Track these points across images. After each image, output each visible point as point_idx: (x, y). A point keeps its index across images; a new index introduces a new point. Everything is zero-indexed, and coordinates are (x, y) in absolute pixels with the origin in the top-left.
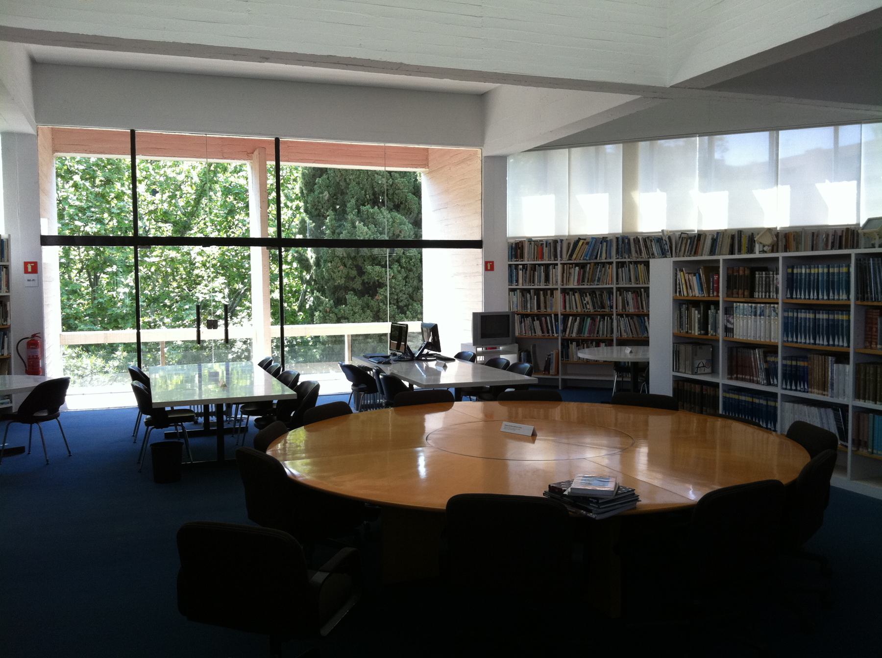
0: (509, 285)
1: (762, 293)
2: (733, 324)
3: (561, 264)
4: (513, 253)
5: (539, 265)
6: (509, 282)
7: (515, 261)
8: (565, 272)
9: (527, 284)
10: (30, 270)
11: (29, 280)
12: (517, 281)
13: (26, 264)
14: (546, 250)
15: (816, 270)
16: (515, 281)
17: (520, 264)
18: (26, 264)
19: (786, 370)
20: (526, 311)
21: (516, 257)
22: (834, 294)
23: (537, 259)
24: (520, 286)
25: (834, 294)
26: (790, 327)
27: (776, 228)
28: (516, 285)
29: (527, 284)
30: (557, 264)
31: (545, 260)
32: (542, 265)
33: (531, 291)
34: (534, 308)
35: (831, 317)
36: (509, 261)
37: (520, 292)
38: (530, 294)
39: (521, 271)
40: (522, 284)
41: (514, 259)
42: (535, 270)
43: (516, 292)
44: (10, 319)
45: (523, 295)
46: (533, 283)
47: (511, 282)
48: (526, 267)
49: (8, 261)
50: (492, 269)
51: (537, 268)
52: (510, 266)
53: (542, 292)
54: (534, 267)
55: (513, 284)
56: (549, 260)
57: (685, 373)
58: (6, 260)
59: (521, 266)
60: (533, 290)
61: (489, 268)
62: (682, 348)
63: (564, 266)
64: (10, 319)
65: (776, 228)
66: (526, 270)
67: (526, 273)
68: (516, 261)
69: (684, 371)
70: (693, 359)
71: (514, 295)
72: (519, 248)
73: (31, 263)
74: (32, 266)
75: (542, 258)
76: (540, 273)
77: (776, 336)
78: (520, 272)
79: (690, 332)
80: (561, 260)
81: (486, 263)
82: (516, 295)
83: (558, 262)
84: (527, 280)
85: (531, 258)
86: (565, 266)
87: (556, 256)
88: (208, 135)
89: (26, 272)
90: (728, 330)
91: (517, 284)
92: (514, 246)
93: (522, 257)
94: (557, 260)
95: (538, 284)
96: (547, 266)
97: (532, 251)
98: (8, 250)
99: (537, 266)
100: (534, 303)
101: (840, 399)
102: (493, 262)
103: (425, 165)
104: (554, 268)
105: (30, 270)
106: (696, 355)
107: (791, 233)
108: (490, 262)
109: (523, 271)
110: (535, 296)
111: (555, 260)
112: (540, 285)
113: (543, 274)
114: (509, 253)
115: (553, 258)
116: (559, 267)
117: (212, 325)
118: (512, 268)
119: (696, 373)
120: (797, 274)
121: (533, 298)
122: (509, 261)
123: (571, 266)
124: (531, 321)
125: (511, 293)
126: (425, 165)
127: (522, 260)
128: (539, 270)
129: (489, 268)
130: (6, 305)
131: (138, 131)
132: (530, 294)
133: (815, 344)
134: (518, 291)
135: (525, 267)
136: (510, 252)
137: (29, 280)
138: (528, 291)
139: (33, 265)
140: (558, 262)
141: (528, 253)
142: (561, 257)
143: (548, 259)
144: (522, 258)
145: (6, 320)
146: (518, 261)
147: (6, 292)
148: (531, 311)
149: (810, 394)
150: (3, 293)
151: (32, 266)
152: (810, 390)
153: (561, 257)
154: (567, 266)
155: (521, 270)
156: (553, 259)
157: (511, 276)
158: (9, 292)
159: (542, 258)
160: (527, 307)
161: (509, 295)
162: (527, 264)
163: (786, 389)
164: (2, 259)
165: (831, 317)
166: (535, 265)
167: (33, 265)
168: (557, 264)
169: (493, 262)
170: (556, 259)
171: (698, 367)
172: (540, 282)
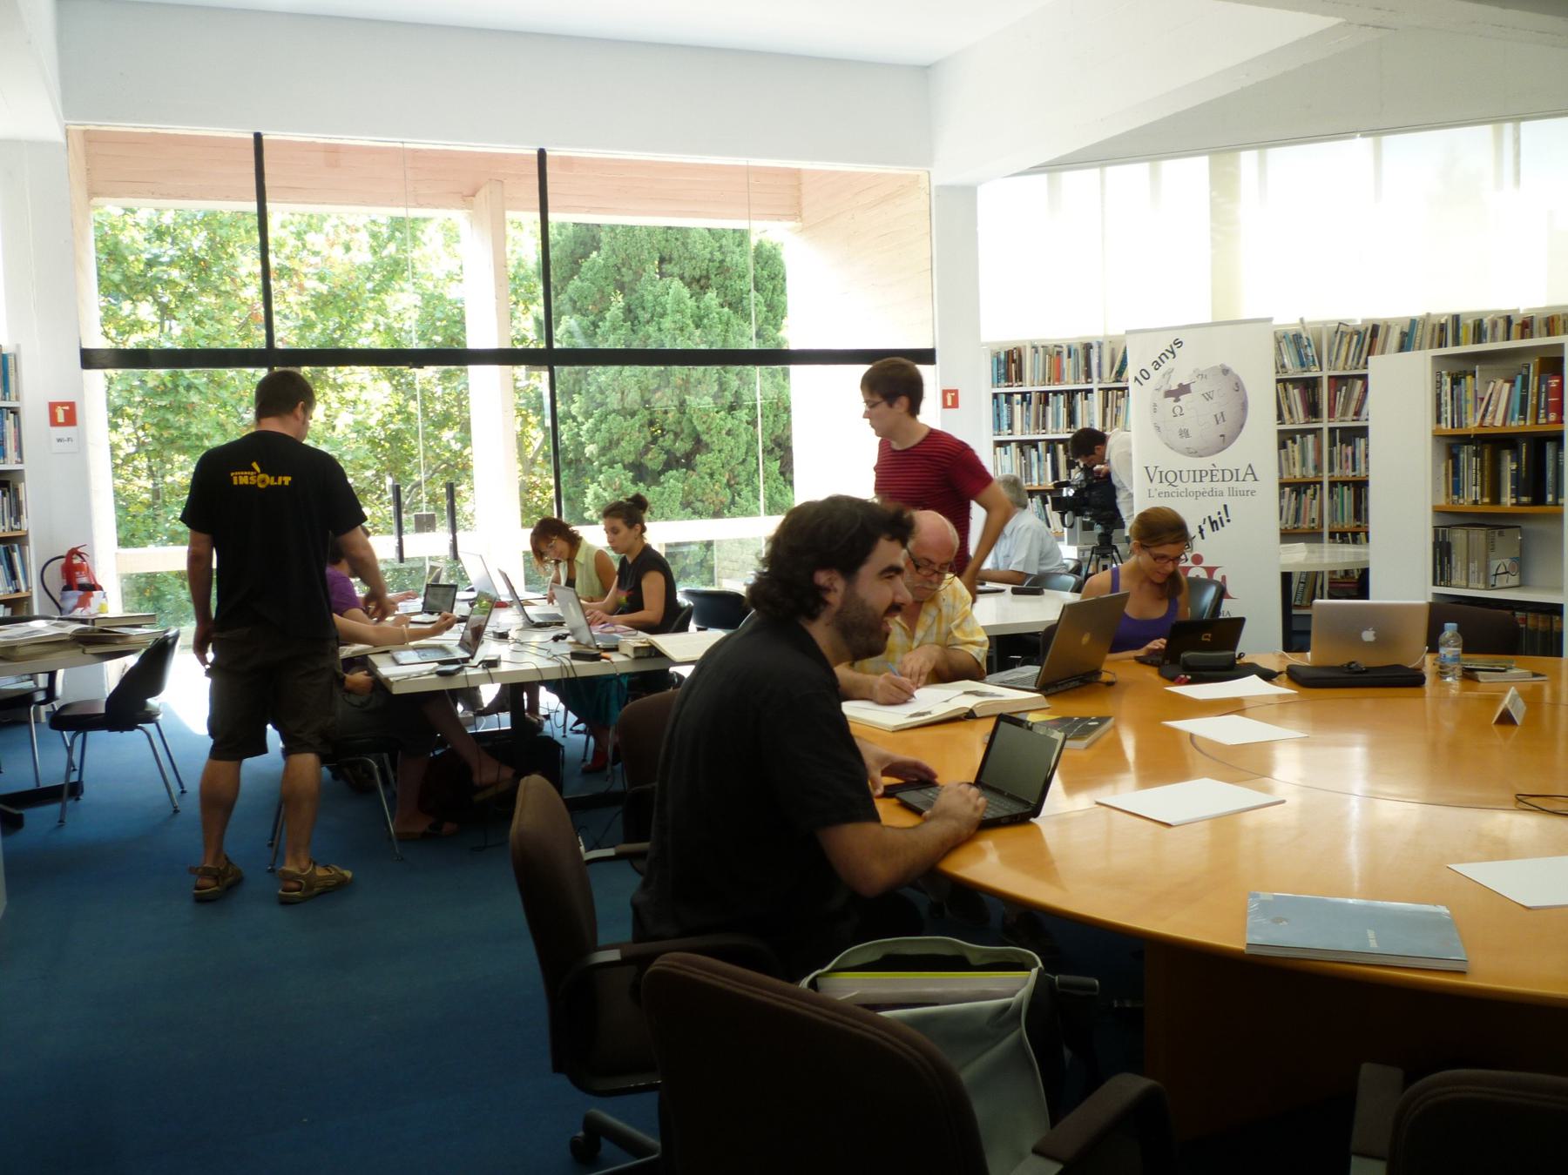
0: (994, 435)
3: (1100, 389)
4: (1002, 371)
5: (1056, 393)
6: (994, 427)
7: (1006, 387)
8: (1110, 405)
9: (1032, 432)
10: (61, 418)
11: (59, 440)
12: (1010, 426)
13: (53, 407)
14: (1067, 364)
16: (1006, 427)
17: (1017, 393)
18: (53, 407)
20: (1029, 483)
21: (1008, 379)
23: (1049, 380)
24: (1018, 436)
27: (1518, 310)
28: (1009, 434)
29: (1032, 432)
30: (1090, 391)
31: (1068, 383)
32: (1061, 392)
33: (1040, 444)
34: (1046, 479)
36: (993, 387)
37: (1017, 447)
38: (1037, 450)
39: (1019, 406)
40: (1022, 430)
41: (1003, 383)
42: (1046, 403)
43: (1008, 448)
44: (27, 518)
45: (1023, 453)
46: (1044, 429)
47: (998, 427)
48: (1028, 399)
49: (17, 399)
50: (955, 404)
51: (1050, 400)
52: (995, 396)
53: (1061, 447)
54: (1044, 398)
55: (1002, 433)
56: (1075, 383)
57: (1467, 587)
58: (13, 398)
59: (1018, 397)
60: (1044, 443)
61: (949, 403)
62: (1459, 537)
63: (1107, 394)
64: (27, 518)
65: (1518, 310)
66: (1030, 403)
67: (1028, 409)
68: (1008, 386)
69: (1464, 583)
70: (1487, 556)
71: (1006, 453)
72: (1014, 361)
73: (62, 404)
74: (64, 410)
75: (1059, 379)
76: (1058, 409)
78: (1017, 408)
80: (1099, 382)
81: (945, 393)
82: (1009, 452)
83: (1095, 386)
84: (1032, 423)
85: (1038, 380)
86: (1110, 393)
87: (1088, 375)
88: (406, 146)
89: (54, 422)
91: (1010, 431)
92: (1002, 356)
93: (1020, 377)
94: (1091, 383)
95: (1054, 430)
96: (1071, 395)
97: (1041, 366)
98: (17, 377)
99: (1050, 394)
100: (1045, 470)
102: (956, 391)
103: (795, 214)
104: (1086, 398)
105: (61, 418)
106: (1493, 550)
107: (1559, 316)
108: (951, 391)
109: (1022, 405)
110: (1049, 455)
111: (1088, 383)
112: (1057, 433)
113: (1063, 412)
114: (992, 370)
115: (1083, 378)
116: (1097, 398)
117: (425, 524)
118: (1000, 401)
119: (1493, 586)
121: (1043, 458)
122: (993, 387)
123: (1120, 393)
124: (1040, 505)
125: (998, 449)
126: (795, 214)
127: (1020, 383)
128: (1055, 404)
129: (949, 403)
130: (16, 490)
131: (267, 137)
132: (1037, 450)
134: (1013, 445)
135: (1024, 394)
136: (995, 369)
137: (59, 440)
138: (1034, 444)
139: (67, 408)
140: (1095, 386)
141: (1033, 370)
142: (1100, 375)
143: (1072, 381)
144: (1021, 380)
145: (18, 520)
146: (1012, 386)
147: (17, 462)
148: (1039, 485)
150: (11, 464)
151: (64, 410)
153: (1100, 375)
154: (1113, 394)
155: (1018, 404)
156: (1084, 381)
157: (998, 416)
158: (22, 463)
159: (1059, 379)
160: (1031, 476)
161: (995, 453)
162: (1030, 393)
164: (4, 394)
166: (1046, 393)
167: (67, 408)
168: (1090, 391)
169: (956, 391)
170: (1089, 380)
171: (1496, 575)
172: (1057, 426)
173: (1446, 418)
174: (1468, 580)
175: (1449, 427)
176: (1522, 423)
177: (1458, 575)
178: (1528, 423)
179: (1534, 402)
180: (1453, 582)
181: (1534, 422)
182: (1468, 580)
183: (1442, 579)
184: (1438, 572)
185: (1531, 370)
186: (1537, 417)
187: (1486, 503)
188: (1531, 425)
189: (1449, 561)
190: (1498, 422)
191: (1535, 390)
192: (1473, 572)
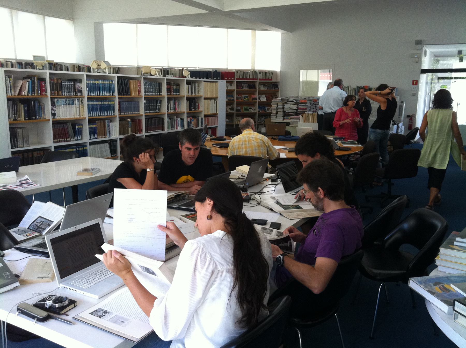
1: (64, 93)
2: (55, 111)
15: (98, 82)
19: (90, 130)
22: (106, 93)
25: (106, 93)
26: (91, 109)
35: (103, 103)
57: (24, 147)
69: (22, 146)
77: (86, 115)
79: (19, 119)
90: (54, 115)
101: (111, 137)
120: (97, 84)
133: (104, 115)
149: (98, 139)
152: (98, 137)
163: (91, 139)
165: (103, 103)
173: (9, 92)
174: (23, 145)
175: (10, 95)
176: (33, 95)
177: (20, 144)
178: (36, 95)
179: (37, 89)
180: (19, 146)
181: (37, 95)
182: (23, 145)
183: (15, 146)
184: (13, 144)
185: (35, 79)
186: (38, 93)
187: (27, 120)
188: (37, 95)
189: (17, 140)
190: (26, 94)
191: (37, 85)
192: (25, 142)
